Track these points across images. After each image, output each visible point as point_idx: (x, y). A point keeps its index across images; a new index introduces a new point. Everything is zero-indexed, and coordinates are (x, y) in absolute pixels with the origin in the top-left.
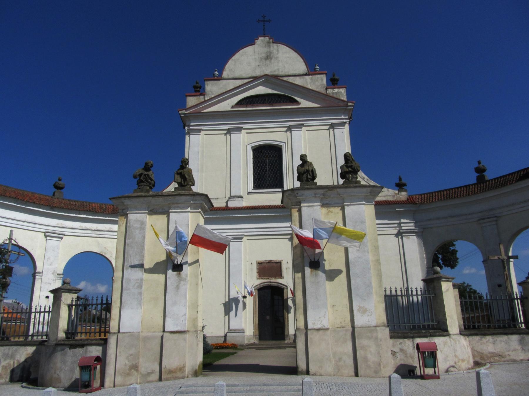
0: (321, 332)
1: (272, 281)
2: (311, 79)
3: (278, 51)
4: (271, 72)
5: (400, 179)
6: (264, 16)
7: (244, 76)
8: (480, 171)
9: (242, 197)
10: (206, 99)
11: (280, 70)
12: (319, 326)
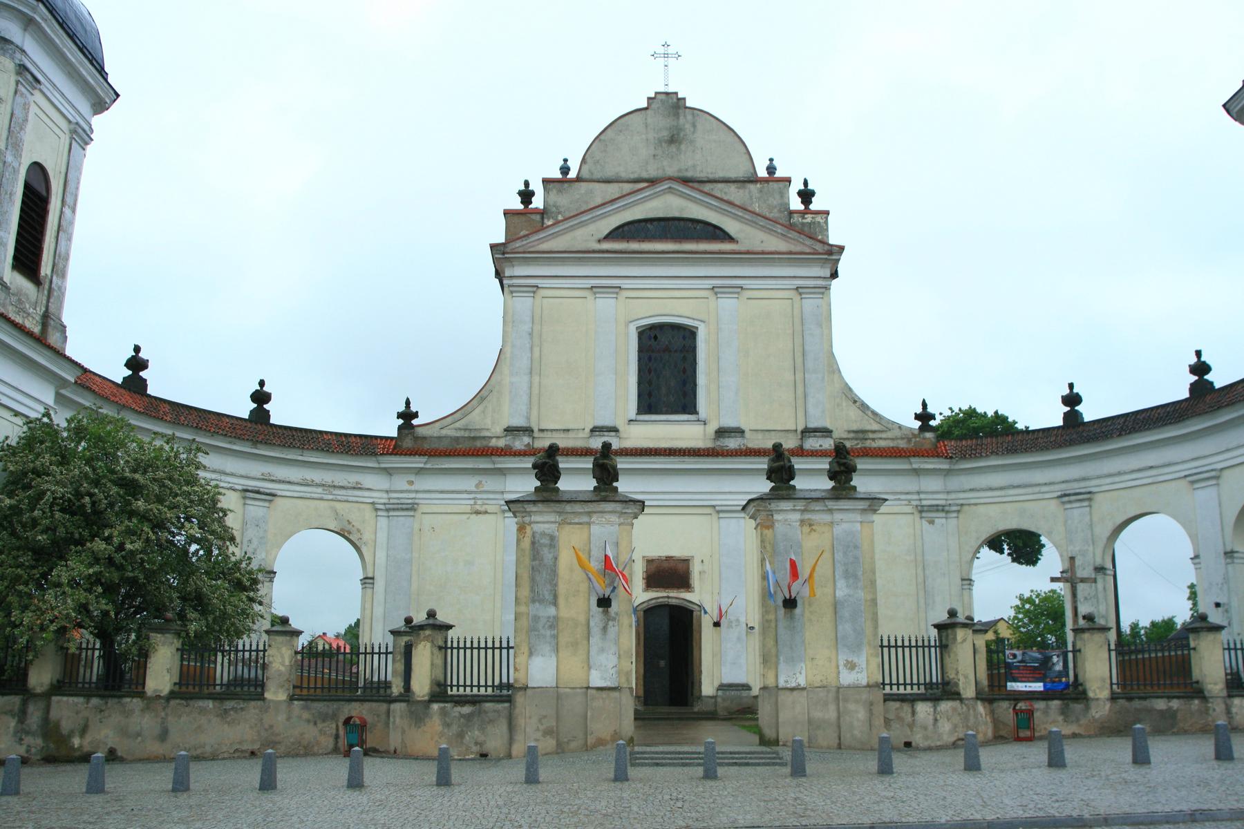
0: (795, 693)
1: (671, 594)
2: (761, 191)
3: (694, 126)
4: (680, 171)
5: (924, 405)
6: (666, 45)
7: (624, 175)
8: (1072, 400)
9: (615, 430)
11: (699, 169)
12: (793, 685)
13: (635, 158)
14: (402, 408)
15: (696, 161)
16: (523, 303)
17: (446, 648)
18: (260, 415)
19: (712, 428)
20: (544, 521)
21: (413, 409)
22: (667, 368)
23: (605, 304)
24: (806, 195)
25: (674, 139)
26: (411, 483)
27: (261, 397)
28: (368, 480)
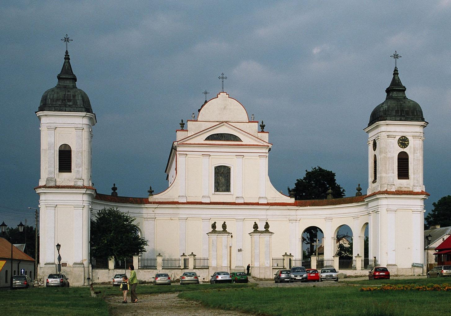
10: (189, 134)
14: (149, 189)
17: (195, 259)
18: (114, 194)
19: (235, 197)
20: (214, 237)
21: (152, 190)
22: (223, 178)
23: (206, 159)
25: (225, 108)
26: (153, 211)
27: (114, 189)
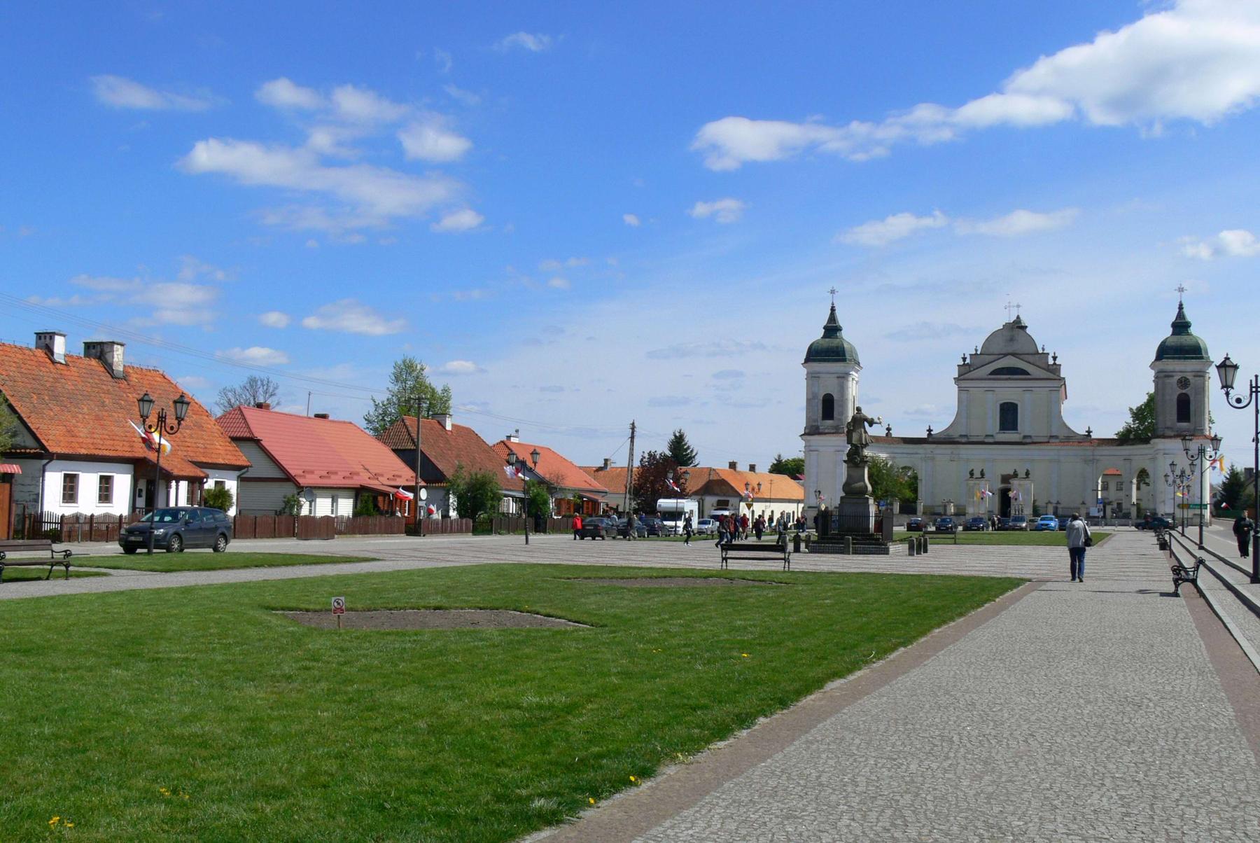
13: (997, 348)
15: (1016, 347)
16: (964, 395)
20: (971, 482)
22: (1009, 415)
23: (990, 395)
24: (1055, 358)
27: (889, 429)
28: (921, 451)
